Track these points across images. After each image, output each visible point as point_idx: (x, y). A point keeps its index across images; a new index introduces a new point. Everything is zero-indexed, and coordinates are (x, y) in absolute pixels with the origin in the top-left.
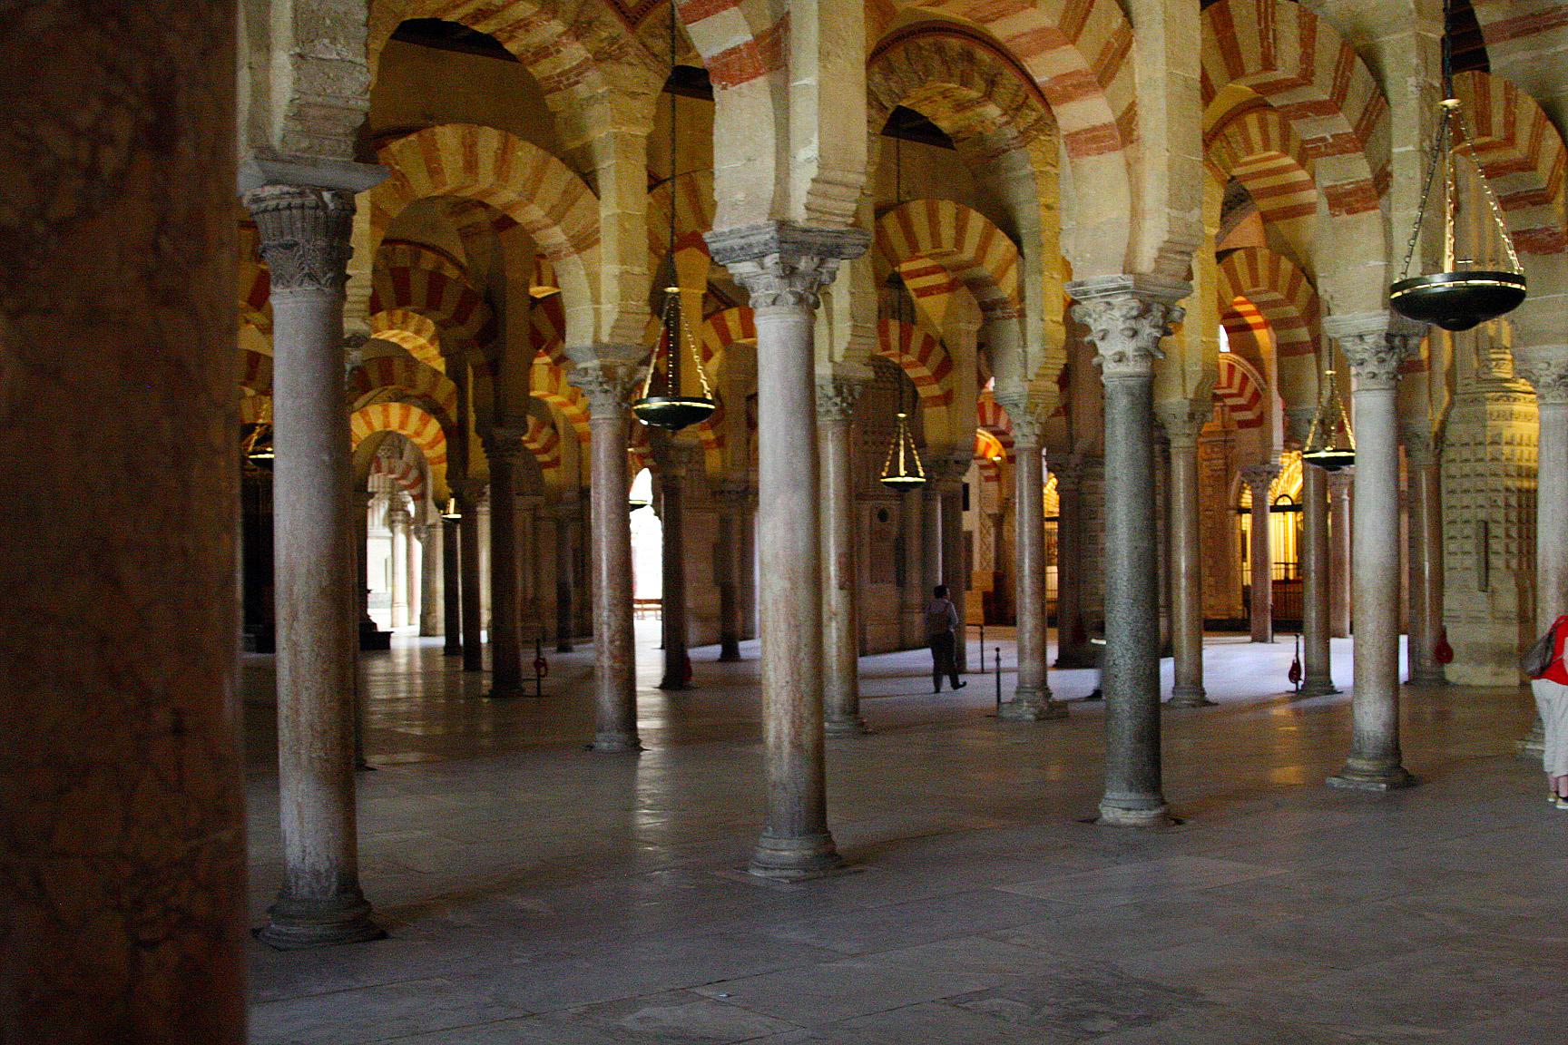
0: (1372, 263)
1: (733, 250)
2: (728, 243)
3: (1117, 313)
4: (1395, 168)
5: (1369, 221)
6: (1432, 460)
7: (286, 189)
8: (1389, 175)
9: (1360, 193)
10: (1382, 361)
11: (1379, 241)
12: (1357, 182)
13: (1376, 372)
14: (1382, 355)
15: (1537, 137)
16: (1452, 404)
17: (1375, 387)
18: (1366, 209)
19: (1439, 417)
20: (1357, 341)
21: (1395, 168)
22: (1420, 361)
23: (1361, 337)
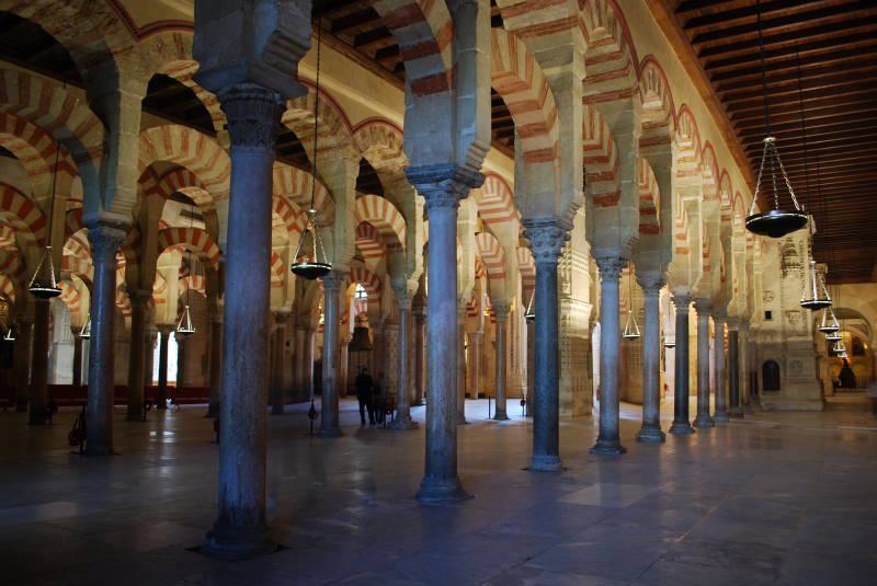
1: (423, 176)
2: (420, 173)
3: (546, 234)
7: (256, 86)
23: (607, 258)
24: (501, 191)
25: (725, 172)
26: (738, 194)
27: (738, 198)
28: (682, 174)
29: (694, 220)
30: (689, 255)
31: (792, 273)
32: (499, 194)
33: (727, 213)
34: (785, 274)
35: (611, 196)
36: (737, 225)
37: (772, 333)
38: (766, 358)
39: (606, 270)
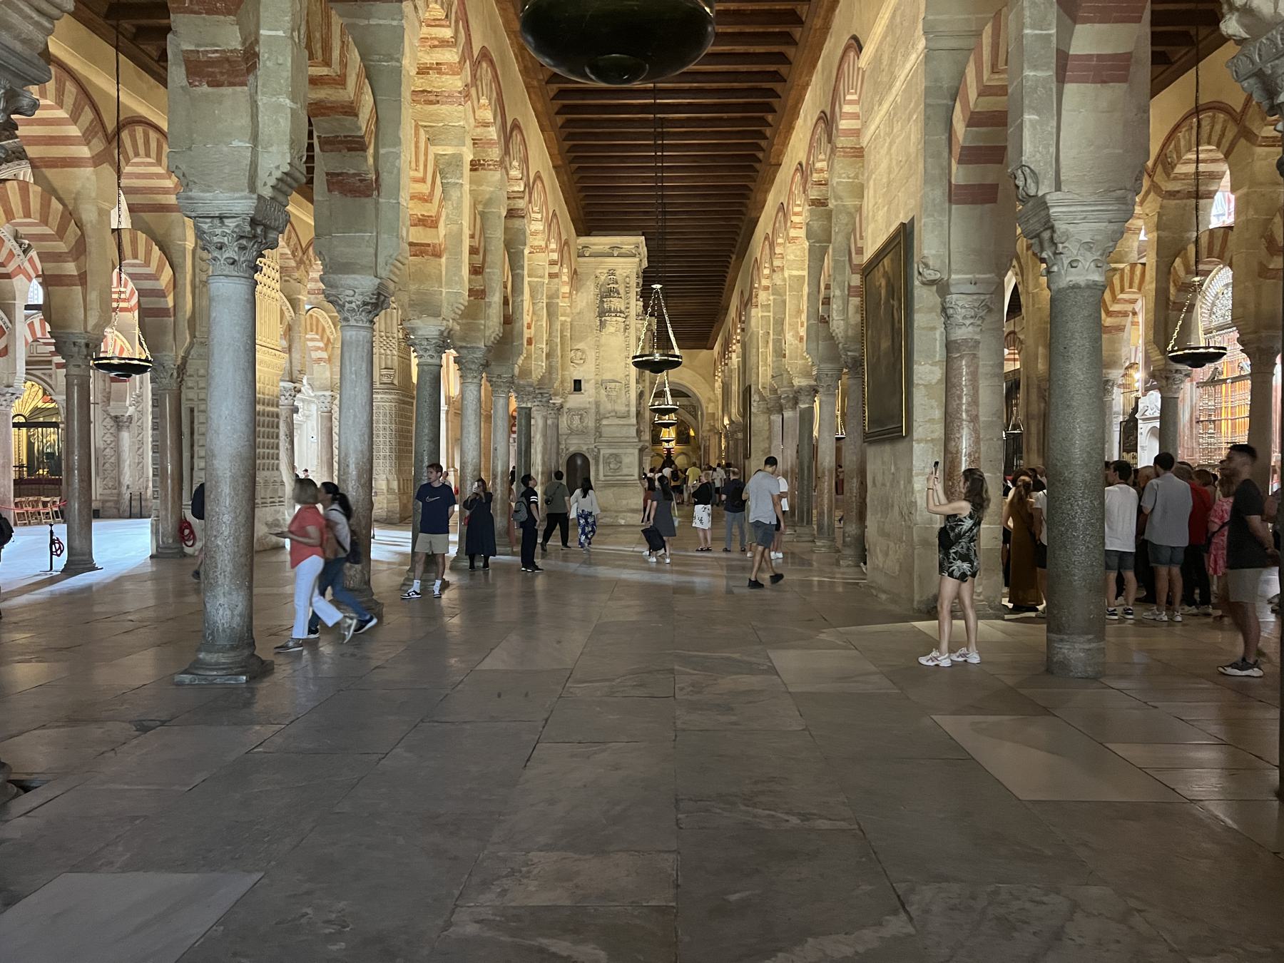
0: (236, 143)
4: (262, 49)
5: (233, 96)
6: (175, 386)
8: (257, 55)
9: (226, 66)
10: (243, 248)
11: (245, 121)
12: (224, 51)
13: (236, 258)
14: (244, 242)
15: (359, 90)
16: (192, 344)
17: (236, 274)
18: (232, 84)
19: (182, 353)
20: (217, 221)
21: (262, 51)
22: (168, 309)
23: (221, 218)
24: (69, 100)
25: (516, 126)
26: (538, 177)
27: (538, 183)
28: (428, 97)
29: (454, 194)
30: (443, 260)
31: (613, 323)
32: (60, 104)
33: (521, 204)
34: (602, 325)
35: (227, 60)
36: (535, 233)
37: (581, 413)
38: (572, 449)
39: (221, 247)
